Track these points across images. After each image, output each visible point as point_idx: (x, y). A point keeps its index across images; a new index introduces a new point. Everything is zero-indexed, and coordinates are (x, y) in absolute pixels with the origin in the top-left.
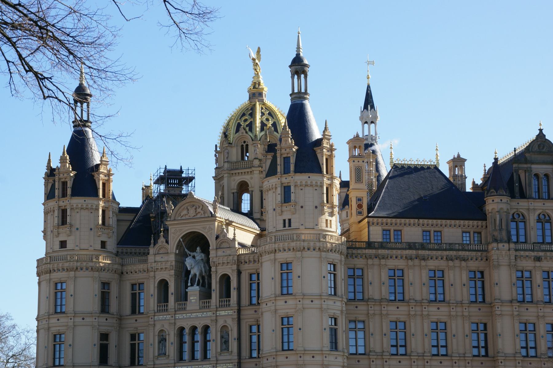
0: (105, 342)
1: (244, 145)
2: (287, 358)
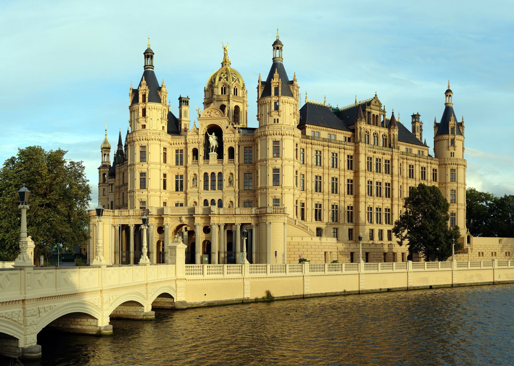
0: (165, 178)
1: (223, 87)
2: (276, 189)
